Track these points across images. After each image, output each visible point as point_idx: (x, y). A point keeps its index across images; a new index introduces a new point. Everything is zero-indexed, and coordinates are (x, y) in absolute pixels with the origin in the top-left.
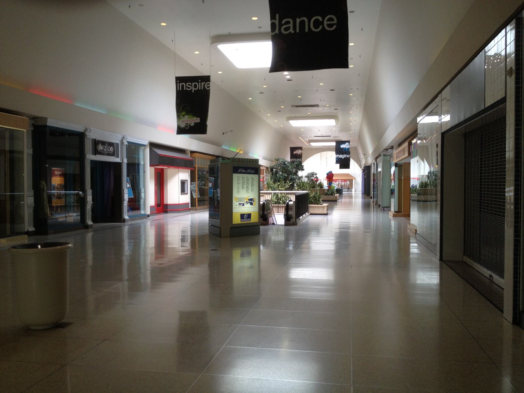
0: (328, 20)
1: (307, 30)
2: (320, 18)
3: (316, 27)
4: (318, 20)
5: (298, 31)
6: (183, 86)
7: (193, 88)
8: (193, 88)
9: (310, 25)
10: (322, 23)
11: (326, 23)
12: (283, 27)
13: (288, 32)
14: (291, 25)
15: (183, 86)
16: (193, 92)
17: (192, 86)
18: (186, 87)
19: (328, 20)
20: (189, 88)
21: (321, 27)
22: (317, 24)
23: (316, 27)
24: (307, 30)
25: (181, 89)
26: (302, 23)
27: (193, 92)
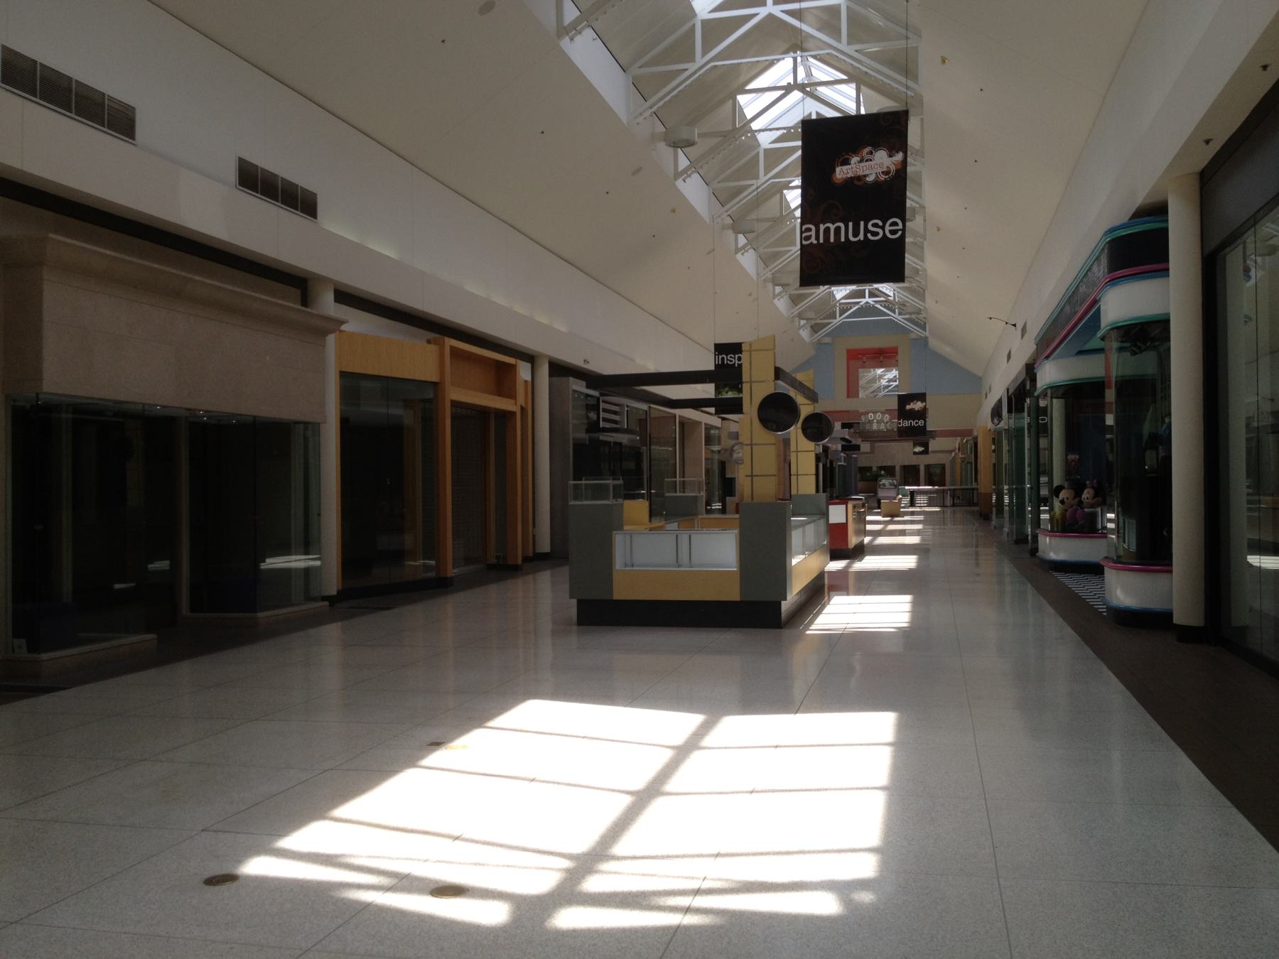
6: (723, 359)
7: (737, 362)
8: (737, 362)
15: (723, 359)
16: (736, 365)
17: (735, 358)
18: (727, 360)
20: (731, 361)
25: (720, 363)
27: (736, 365)
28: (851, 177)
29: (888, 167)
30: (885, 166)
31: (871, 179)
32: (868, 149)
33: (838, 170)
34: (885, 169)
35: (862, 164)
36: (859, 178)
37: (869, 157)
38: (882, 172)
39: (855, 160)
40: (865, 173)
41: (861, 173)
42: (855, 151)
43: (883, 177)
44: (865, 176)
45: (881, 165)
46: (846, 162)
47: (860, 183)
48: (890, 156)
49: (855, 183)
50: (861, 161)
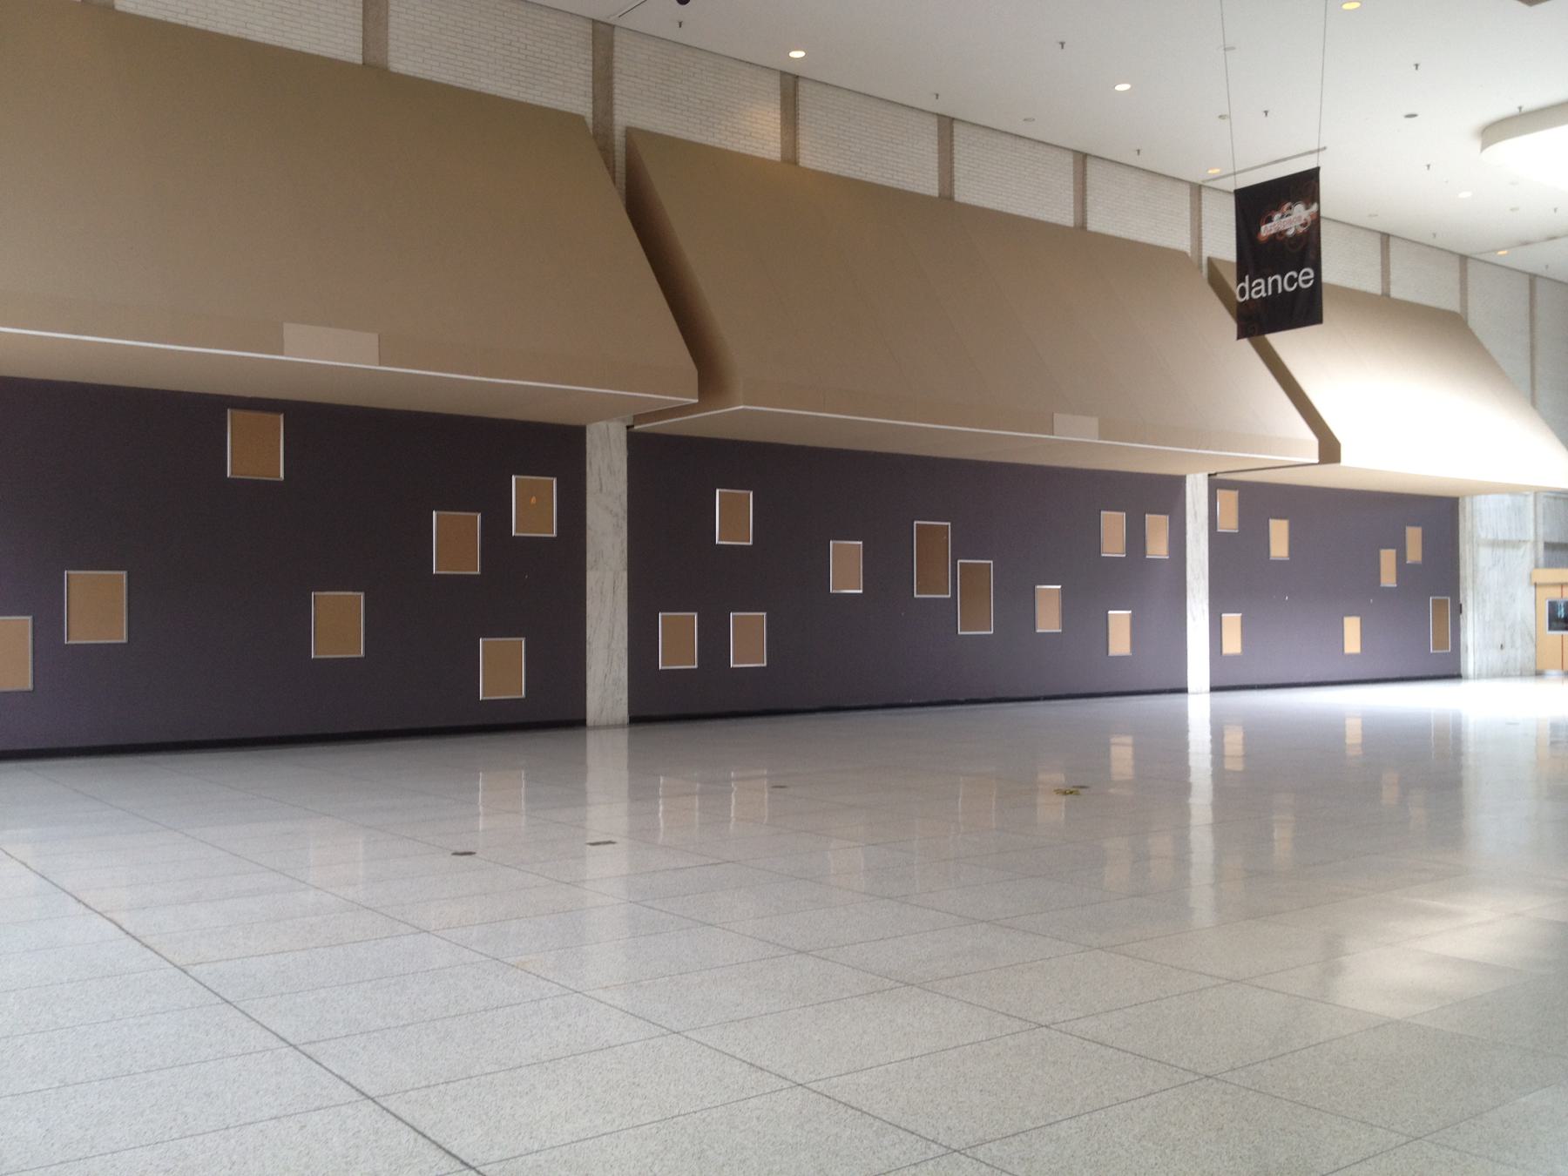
0: (1303, 275)
1: (1280, 291)
2: (1294, 274)
3: (1291, 285)
4: (1291, 277)
5: (1270, 293)
9: (1283, 285)
10: (1297, 280)
11: (1301, 279)
12: (1254, 291)
13: (1259, 296)
14: (1263, 287)
19: (1303, 275)
22: (1292, 281)
23: (1291, 285)
24: (1280, 291)
26: (1275, 282)
28: (1274, 234)
29: (1305, 220)
30: (1303, 218)
31: (1290, 233)
34: (1303, 222)
35: (1283, 220)
36: (1281, 233)
37: (1289, 212)
38: (1301, 225)
39: (1277, 216)
40: (1285, 228)
41: (1282, 228)
42: (1277, 208)
43: (1301, 230)
44: (1286, 230)
46: (1269, 220)
47: (1282, 238)
49: (1278, 237)
50: (1282, 217)
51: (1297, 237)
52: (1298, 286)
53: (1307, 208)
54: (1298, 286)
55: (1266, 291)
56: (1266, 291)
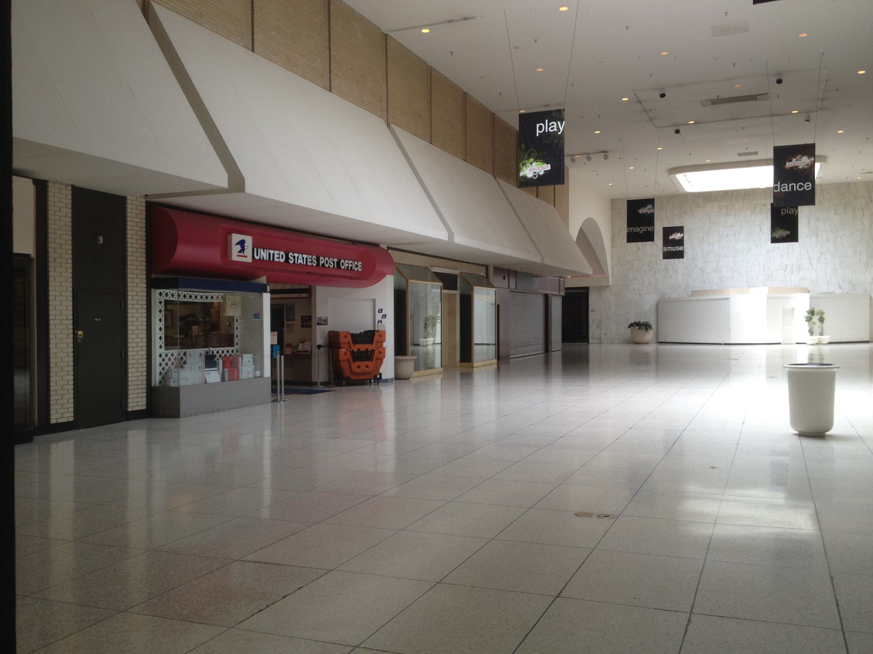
0: (807, 185)
1: (795, 190)
4: (801, 185)
5: (790, 190)
9: (796, 187)
10: (803, 186)
11: (805, 186)
12: (782, 188)
19: (807, 185)
21: (803, 188)
22: (800, 187)
24: (795, 190)
26: (793, 186)
31: (801, 167)
32: (800, 156)
33: (787, 164)
34: (807, 164)
36: (796, 167)
37: (800, 159)
38: (806, 165)
42: (795, 157)
43: (806, 167)
45: (805, 162)
46: (791, 161)
48: (809, 159)
50: (797, 160)
51: (804, 170)
52: (804, 189)
53: (809, 159)
54: (804, 189)
55: (788, 189)
56: (788, 189)
